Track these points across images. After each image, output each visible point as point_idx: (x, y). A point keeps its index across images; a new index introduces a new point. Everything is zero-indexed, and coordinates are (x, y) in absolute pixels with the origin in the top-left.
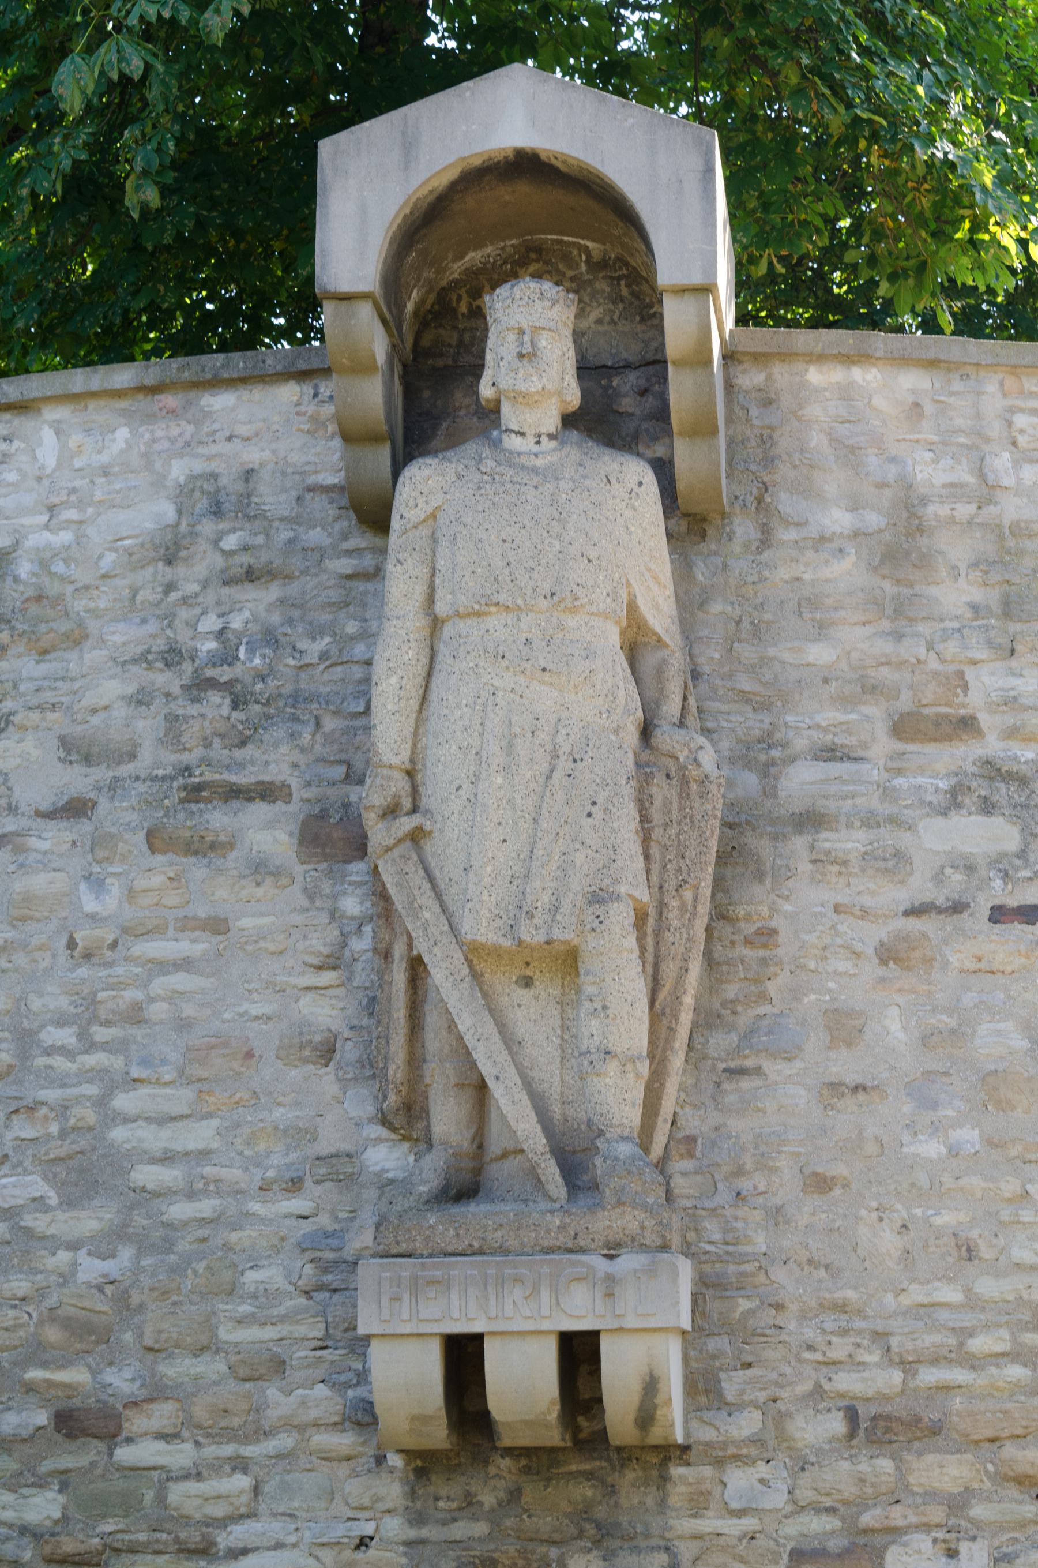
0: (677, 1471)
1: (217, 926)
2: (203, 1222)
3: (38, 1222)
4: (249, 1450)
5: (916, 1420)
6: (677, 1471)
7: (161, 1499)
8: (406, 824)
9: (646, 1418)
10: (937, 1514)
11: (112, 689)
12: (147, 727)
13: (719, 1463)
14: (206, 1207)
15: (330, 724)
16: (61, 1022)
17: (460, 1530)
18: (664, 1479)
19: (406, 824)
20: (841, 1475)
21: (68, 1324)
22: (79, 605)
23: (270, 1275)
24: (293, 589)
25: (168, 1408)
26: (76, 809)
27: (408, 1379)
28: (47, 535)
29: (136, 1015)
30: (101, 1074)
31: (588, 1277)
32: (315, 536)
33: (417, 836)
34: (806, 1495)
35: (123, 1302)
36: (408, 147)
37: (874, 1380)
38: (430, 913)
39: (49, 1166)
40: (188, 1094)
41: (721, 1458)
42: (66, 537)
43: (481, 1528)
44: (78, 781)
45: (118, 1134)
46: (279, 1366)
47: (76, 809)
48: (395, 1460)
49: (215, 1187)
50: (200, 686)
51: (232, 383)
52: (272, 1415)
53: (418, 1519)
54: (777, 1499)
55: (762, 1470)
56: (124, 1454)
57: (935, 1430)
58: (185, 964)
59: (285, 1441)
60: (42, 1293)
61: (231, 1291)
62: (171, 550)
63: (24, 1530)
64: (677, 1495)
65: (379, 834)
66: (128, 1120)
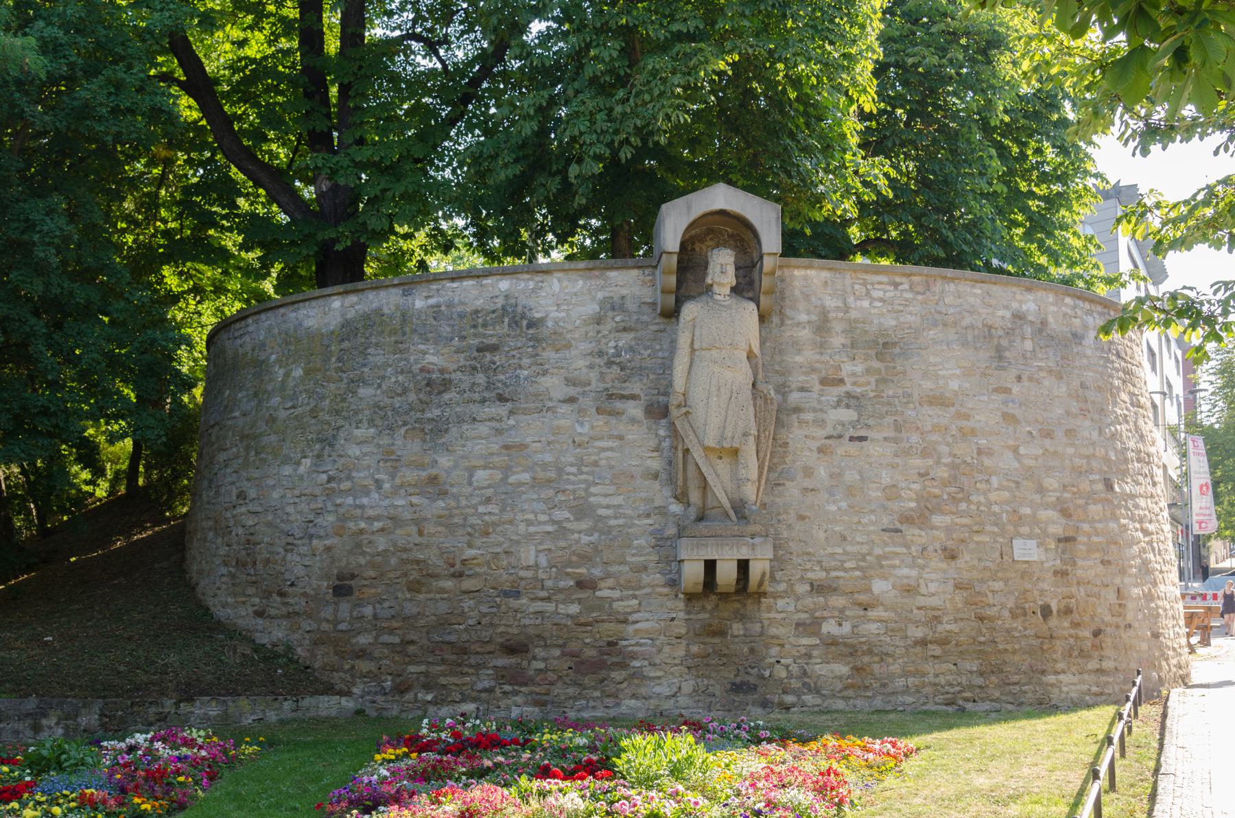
0: (763, 600)
1: (621, 438)
2: (620, 526)
3: (568, 525)
4: (637, 593)
5: (830, 587)
6: (763, 600)
7: (611, 606)
8: (684, 410)
9: (761, 584)
10: (837, 614)
11: (581, 363)
12: (594, 375)
13: (775, 598)
14: (621, 522)
15: (652, 377)
16: (572, 465)
17: (701, 616)
18: (760, 602)
19: (684, 410)
20: (809, 602)
21: (579, 555)
22: (569, 336)
23: (641, 542)
24: (638, 334)
25: (612, 580)
26: (571, 400)
27: (693, 573)
28: (557, 314)
29: (596, 464)
30: (586, 481)
31: (747, 544)
32: (645, 318)
33: (687, 413)
34: (799, 607)
35: (596, 549)
36: (689, 208)
37: (818, 575)
38: (692, 437)
39: (570, 509)
40: (614, 488)
41: (776, 596)
42: (563, 314)
43: (707, 616)
44: (572, 391)
45: (592, 499)
46: (646, 568)
47: (571, 400)
48: (681, 596)
49: (624, 516)
50: (610, 364)
51: (617, 269)
52: (644, 582)
53: (688, 613)
54: (792, 608)
55: (787, 600)
56: (598, 593)
57: (835, 590)
58: (611, 449)
59: (648, 590)
60: (570, 546)
61: (629, 547)
62: (598, 320)
63: (568, 616)
64: (763, 606)
65: (674, 412)
66: (595, 495)
